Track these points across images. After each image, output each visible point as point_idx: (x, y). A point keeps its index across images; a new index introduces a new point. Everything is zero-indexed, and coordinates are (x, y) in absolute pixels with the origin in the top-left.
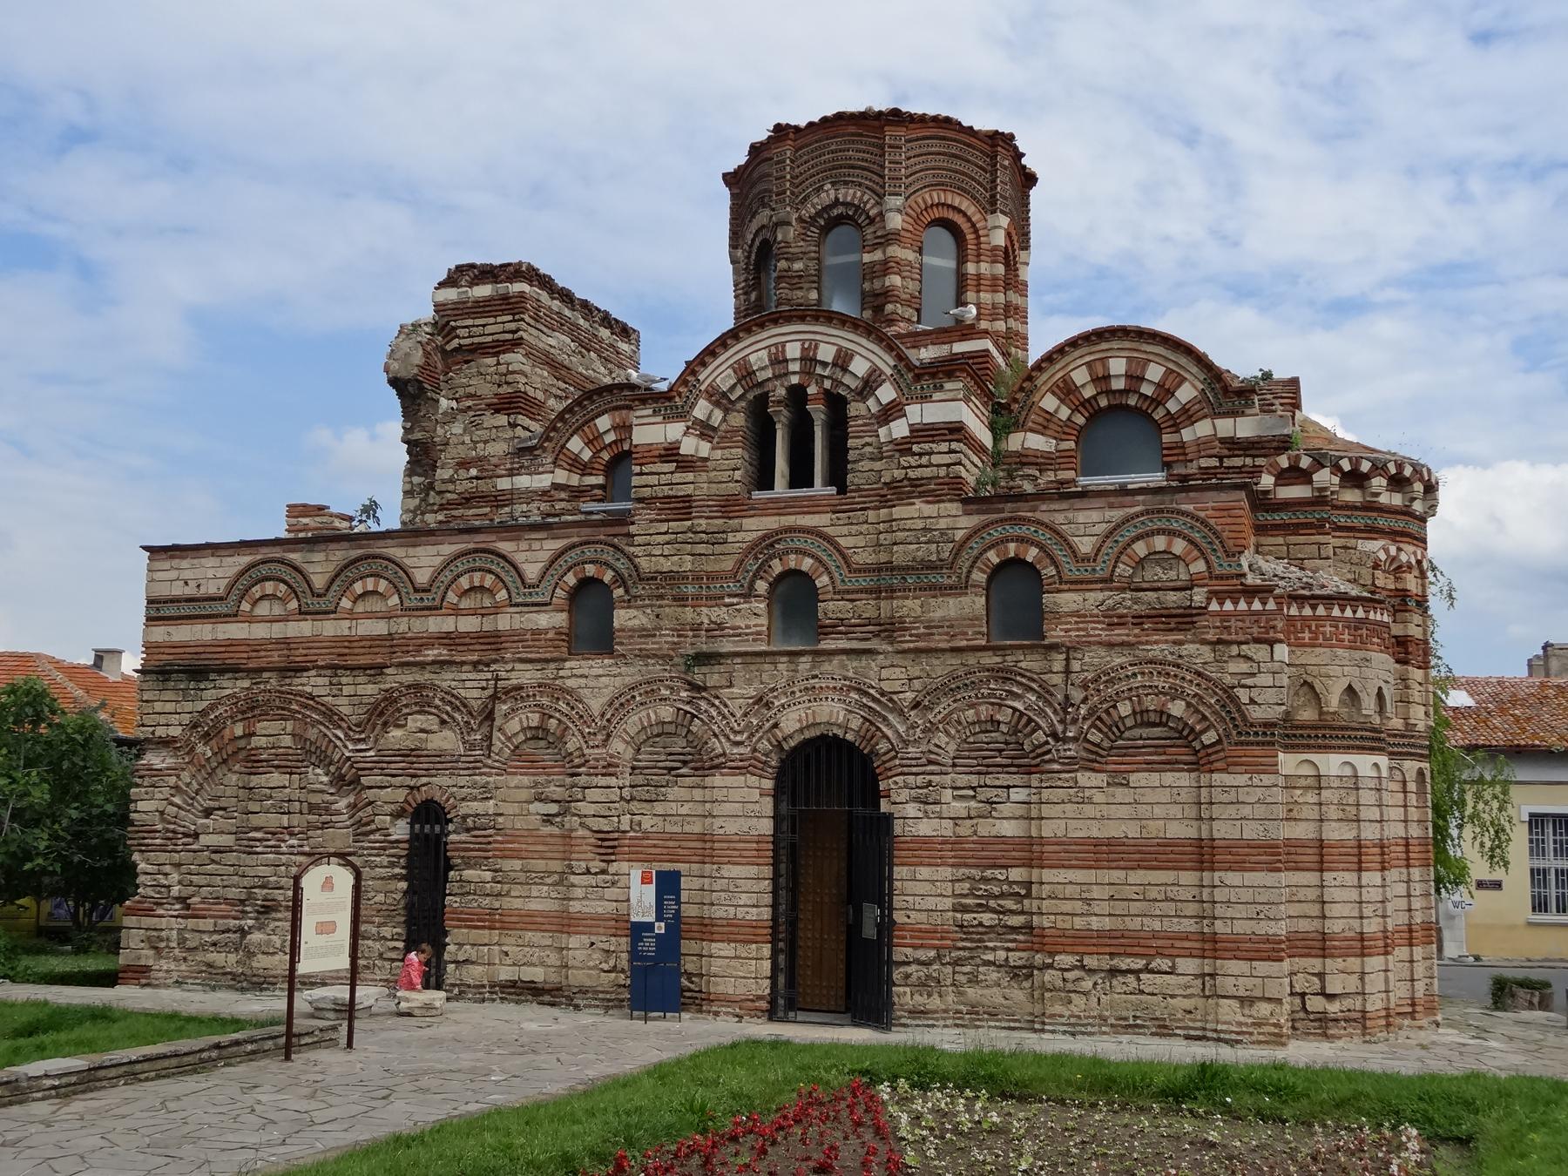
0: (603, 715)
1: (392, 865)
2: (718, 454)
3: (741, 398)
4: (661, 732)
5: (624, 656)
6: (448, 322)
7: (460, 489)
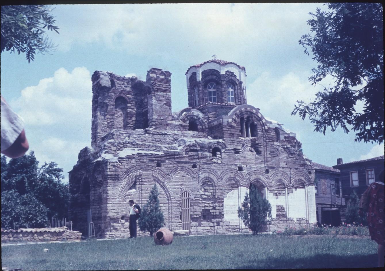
0: (220, 175)
1: (178, 206)
2: (237, 126)
3: (240, 116)
4: (230, 179)
5: (224, 163)
6: (154, 82)
7: (159, 121)
